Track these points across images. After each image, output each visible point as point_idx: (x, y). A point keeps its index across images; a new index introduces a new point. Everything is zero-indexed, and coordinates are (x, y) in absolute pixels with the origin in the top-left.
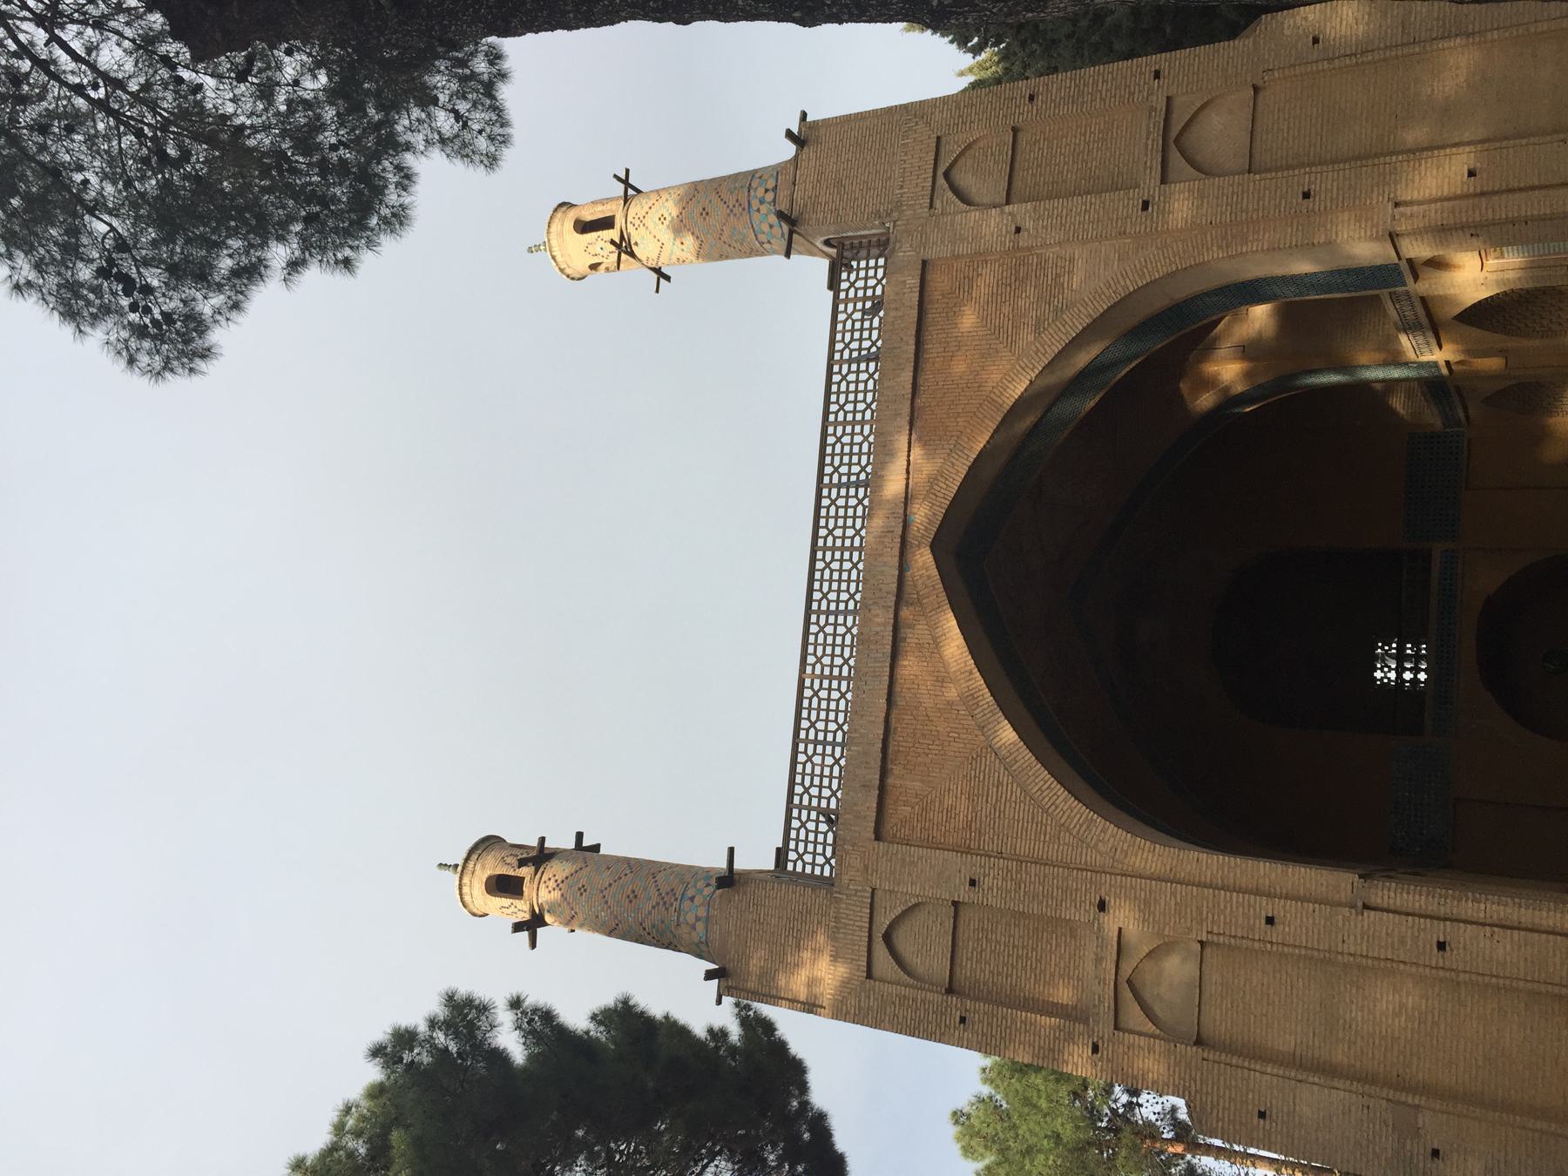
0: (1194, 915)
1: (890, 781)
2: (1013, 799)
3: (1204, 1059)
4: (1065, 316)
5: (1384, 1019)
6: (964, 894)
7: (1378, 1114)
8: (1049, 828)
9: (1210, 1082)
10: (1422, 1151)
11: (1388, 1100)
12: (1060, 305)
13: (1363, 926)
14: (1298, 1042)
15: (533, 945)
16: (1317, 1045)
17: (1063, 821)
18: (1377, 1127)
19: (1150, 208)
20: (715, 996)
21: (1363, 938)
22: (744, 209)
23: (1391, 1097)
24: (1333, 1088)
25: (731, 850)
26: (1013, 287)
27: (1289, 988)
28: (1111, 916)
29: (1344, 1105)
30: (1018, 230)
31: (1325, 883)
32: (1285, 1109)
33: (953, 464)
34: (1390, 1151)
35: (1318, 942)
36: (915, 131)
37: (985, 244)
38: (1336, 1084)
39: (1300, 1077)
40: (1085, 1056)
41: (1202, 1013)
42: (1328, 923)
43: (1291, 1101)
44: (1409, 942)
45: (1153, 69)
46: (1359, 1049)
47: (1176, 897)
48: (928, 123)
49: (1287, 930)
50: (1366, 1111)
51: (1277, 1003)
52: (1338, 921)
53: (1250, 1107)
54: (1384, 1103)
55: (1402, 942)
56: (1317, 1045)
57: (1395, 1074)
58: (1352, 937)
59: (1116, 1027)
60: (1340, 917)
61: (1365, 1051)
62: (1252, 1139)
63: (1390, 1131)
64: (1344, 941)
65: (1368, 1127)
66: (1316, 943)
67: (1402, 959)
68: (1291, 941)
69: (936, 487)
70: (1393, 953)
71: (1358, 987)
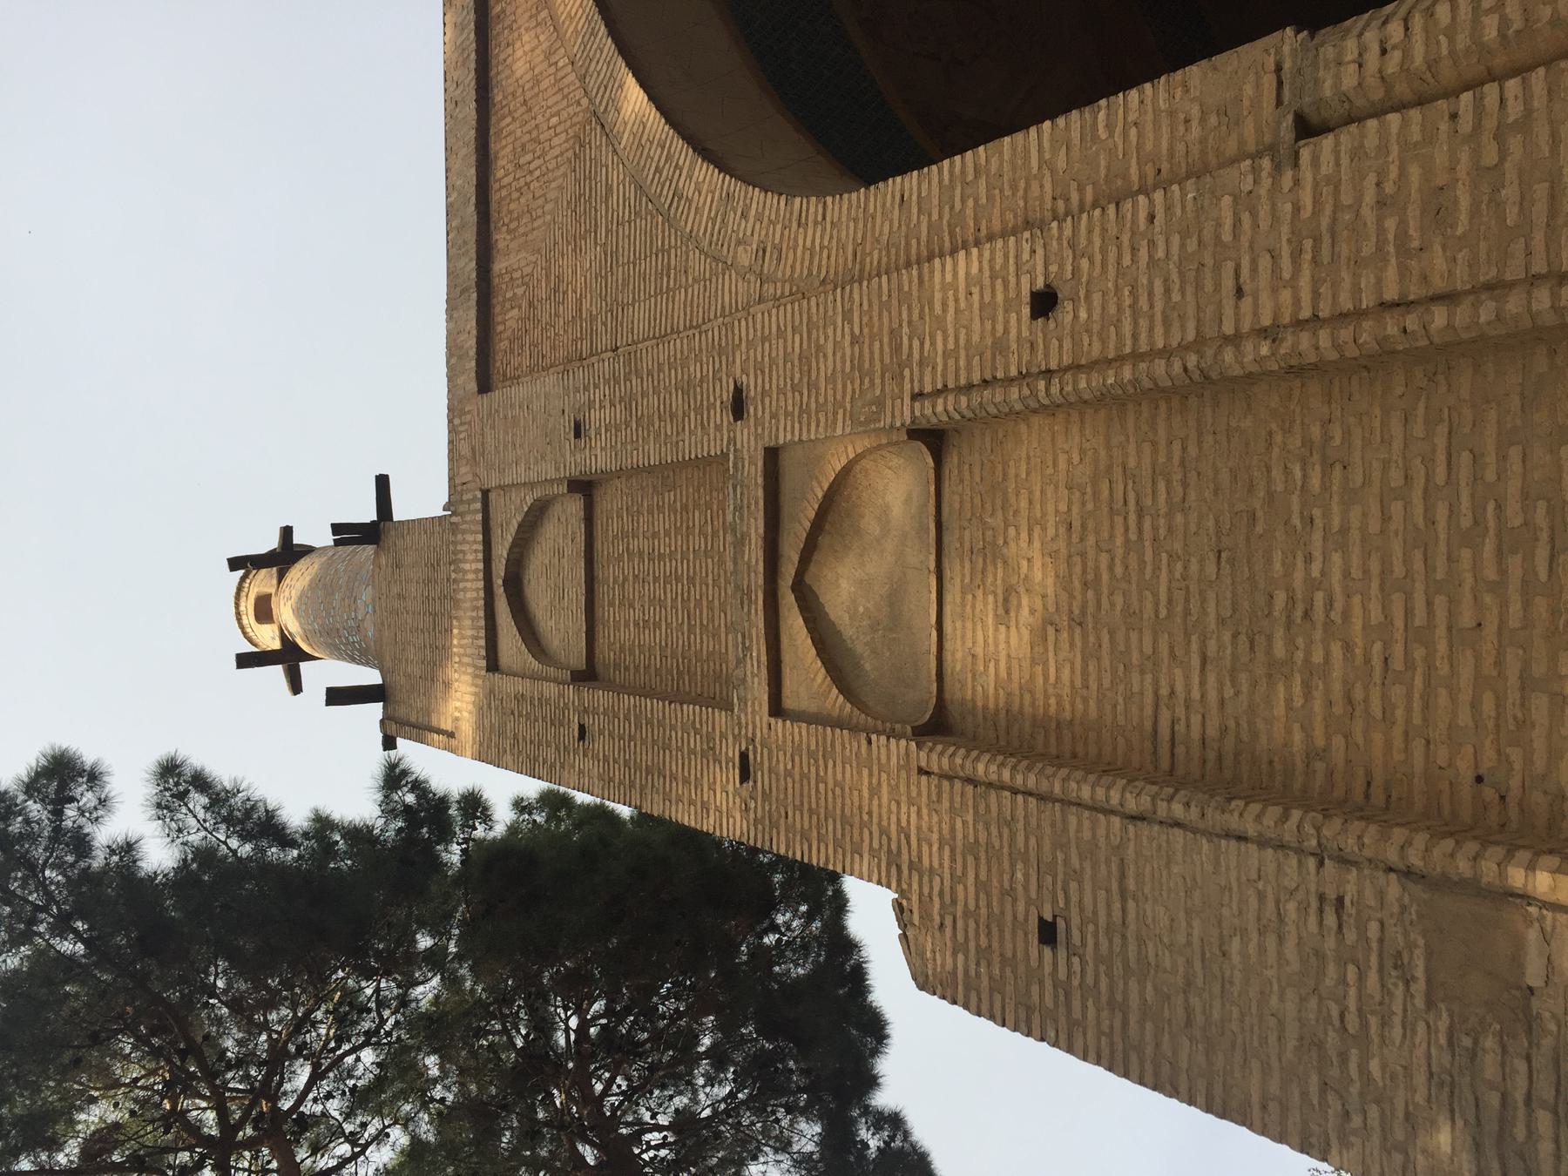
0: (887, 360)
1: (499, 266)
3: (921, 771)
5: (1418, 565)
6: (577, 461)
7: (1373, 930)
9: (935, 837)
11: (1408, 873)
13: (1297, 209)
14: (1164, 691)
16: (1212, 696)
18: (1373, 978)
20: (379, 737)
21: (1296, 255)
23: (1415, 859)
24: (1228, 835)
25: (382, 483)
27: (1132, 517)
29: (1261, 896)
31: (1195, 111)
32: (1102, 920)
34: (1420, 1079)
35: (1167, 323)
38: (1233, 821)
39: (1131, 805)
40: (730, 788)
41: (948, 645)
42: (1192, 245)
43: (1115, 886)
44: (1464, 202)
46: (1337, 687)
47: (851, 322)
49: (1083, 315)
50: (1330, 919)
51: (1105, 577)
52: (1219, 225)
53: (1021, 908)
54: (1394, 888)
55: (1438, 212)
56: (1212, 696)
57: (1467, 776)
58: (1265, 262)
59: (777, 708)
60: (1227, 201)
61: (1358, 694)
62: (1029, 1010)
63: (1419, 1002)
64: (1239, 292)
65: (1343, 980)
66: (1159, 330)
67: (1439, 285)
68: (1096, 352)
70: (1403, 271)
71: (1327, 466)
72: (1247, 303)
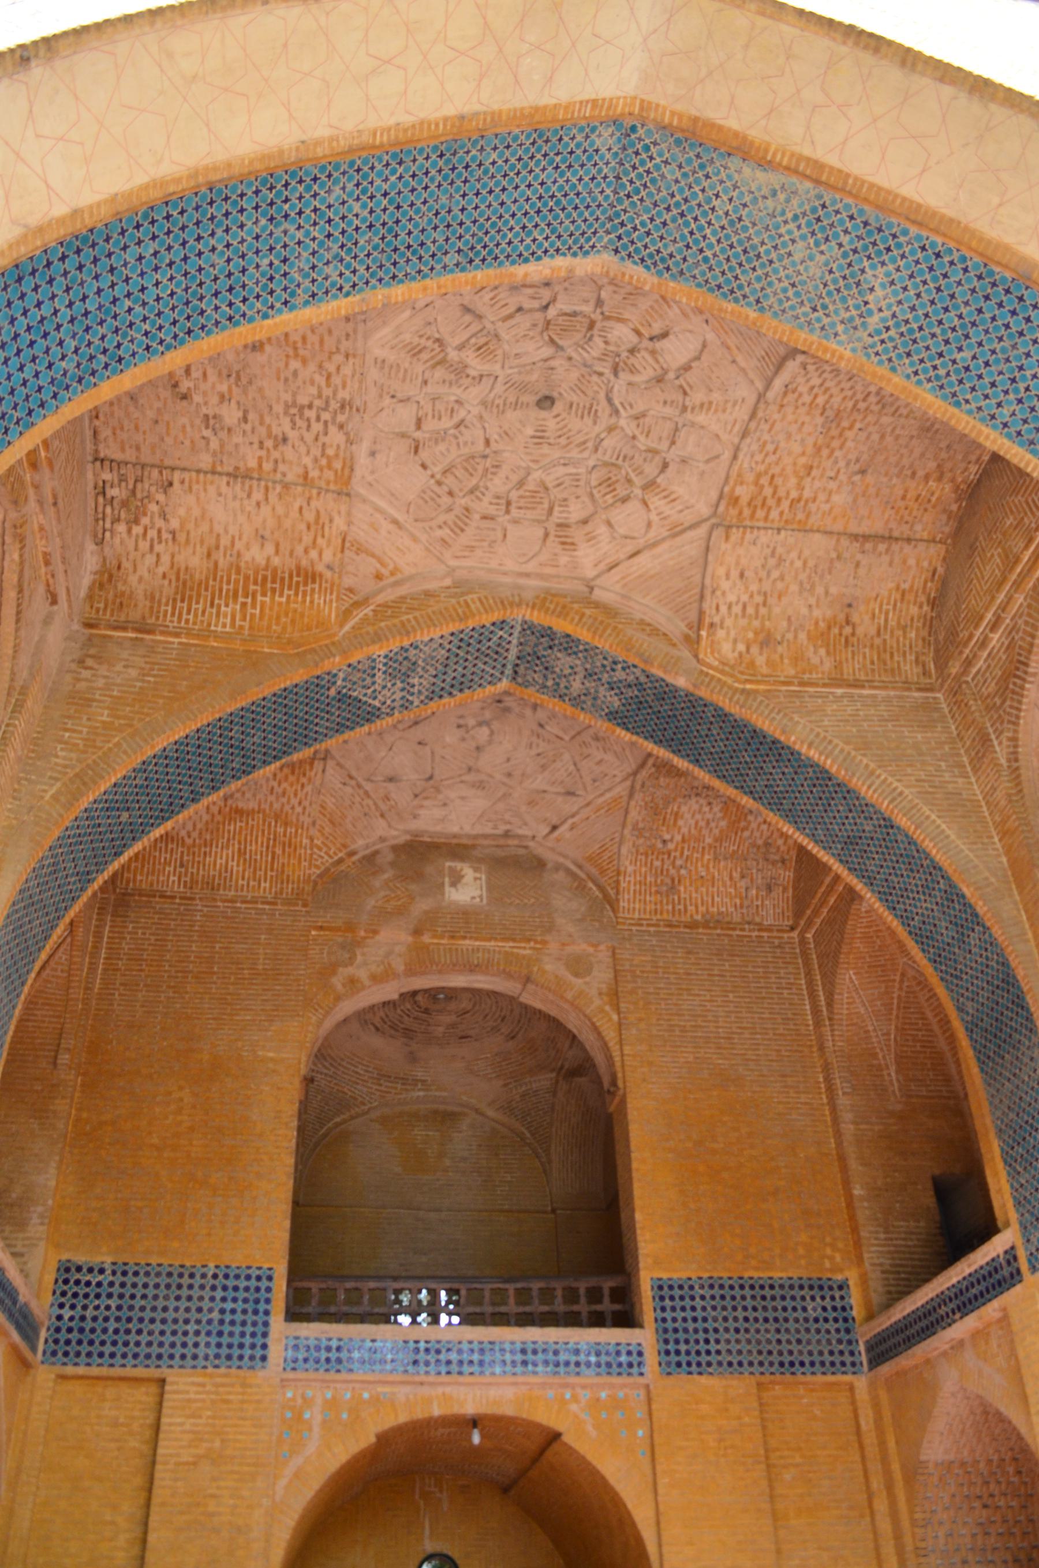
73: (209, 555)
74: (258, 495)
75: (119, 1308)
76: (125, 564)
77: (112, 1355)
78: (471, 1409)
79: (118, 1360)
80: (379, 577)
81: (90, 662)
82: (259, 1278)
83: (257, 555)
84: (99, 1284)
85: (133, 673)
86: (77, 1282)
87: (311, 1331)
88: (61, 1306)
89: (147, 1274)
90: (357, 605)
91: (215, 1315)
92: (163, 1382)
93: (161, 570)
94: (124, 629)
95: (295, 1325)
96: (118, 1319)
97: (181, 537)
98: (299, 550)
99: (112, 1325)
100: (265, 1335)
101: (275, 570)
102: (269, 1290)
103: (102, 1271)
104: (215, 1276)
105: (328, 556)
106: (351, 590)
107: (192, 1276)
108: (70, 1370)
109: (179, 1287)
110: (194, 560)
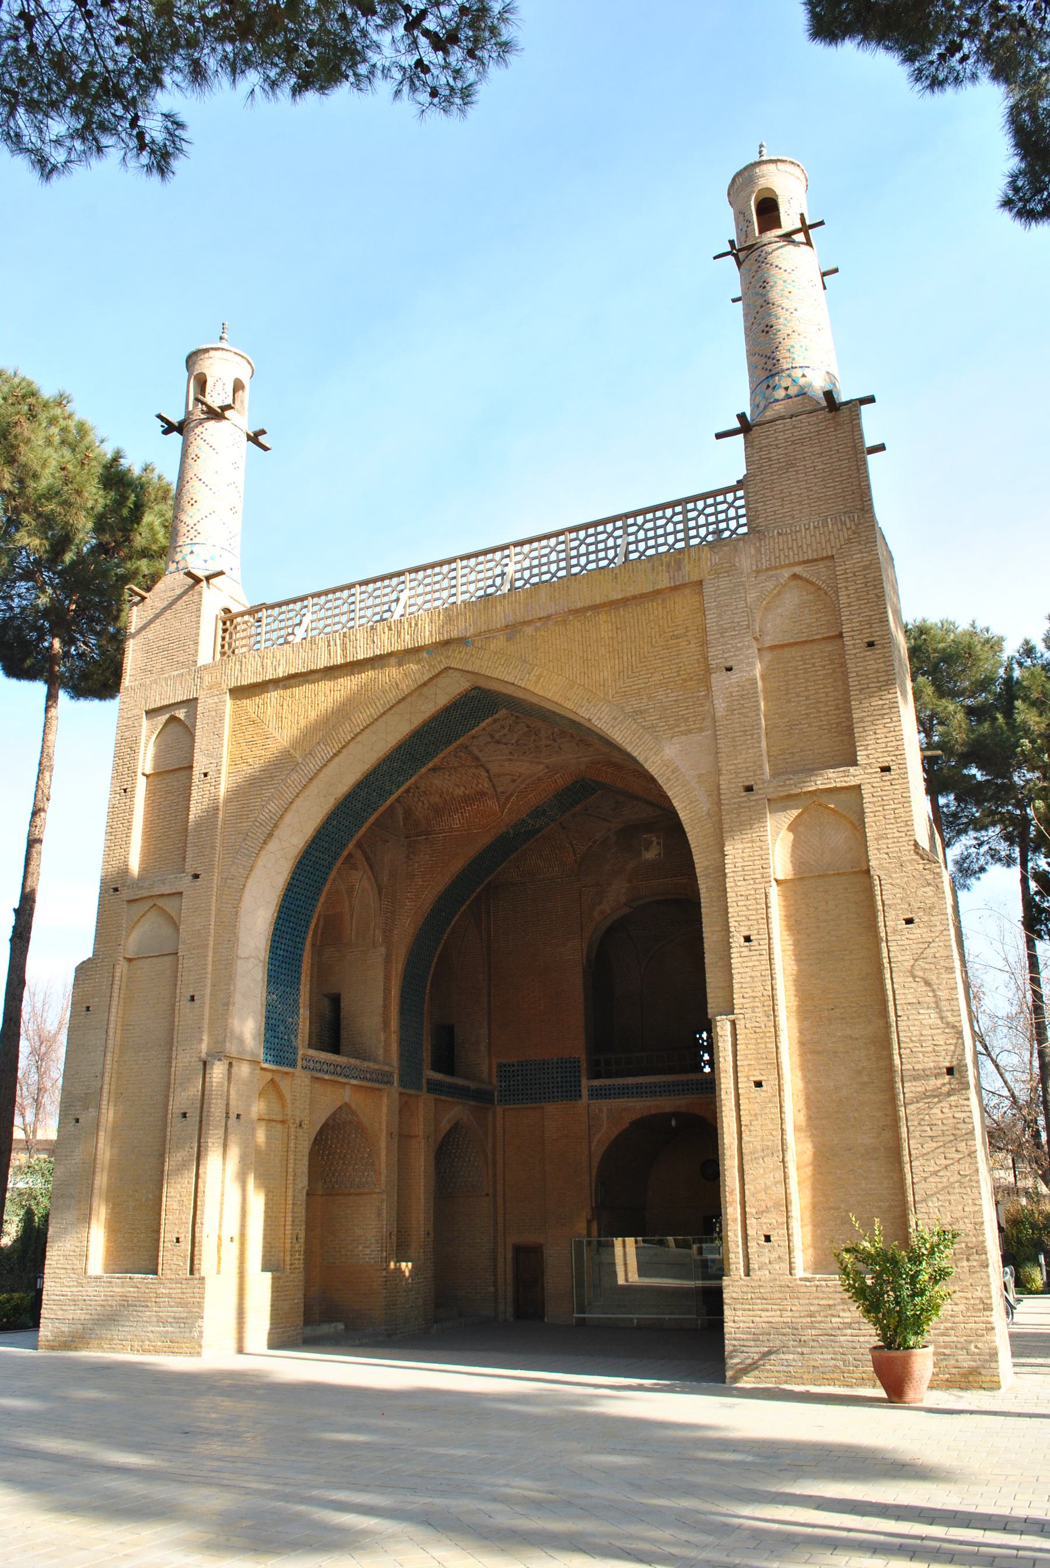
2: (263, 792)
4: (648, 735)
8: (246, 824)
10: (77, 1112)
12: (657, 729)
15: (166, 432)
17: (249, 834)
19: (744, 794)
22: (770, 370)
26: (676, 679)
28: (192, 884)
30: (729, 669)
33: (516, 667)
36: (842, 530)
37: (715, 639)
45: (891, 763)
48: (849, 541)
69: (496, 658)
72: (182, 1052)
73: (441, 796)
74: (447, 773)
75: (522, 1080)
76: (412, 808)
77: (523, 1099)
78: (667, 1110)
79: (525, 1101)
80: (514, 781)
81: (411, 856)
82: (574, 1062)
83: (459, 792)
84: (513, 1071)
85: (427, 857)
86: (505, 1071)
87: (596, 1083)
88: (501, 1082)
89: (531, 1065)
90: (508, 798)
91: (559, 1079)
92: (542, 1108)
93: (426, 806)
94: (420, 836)
95: (591, 1081)
96: (522, 1085)
97: (428, 793)
98: (474, 786)
99: (521, 1087)
100: (580, 1086)
101: (468, 795)
102: (579, 1067)
103: (513, 1066)
104: (557, 1063)
105: (486, 785)
106: (503, 793)
107: (548, 1064)
108: (508, 1106)
109: (544, 1069)
110: (436, 799)
